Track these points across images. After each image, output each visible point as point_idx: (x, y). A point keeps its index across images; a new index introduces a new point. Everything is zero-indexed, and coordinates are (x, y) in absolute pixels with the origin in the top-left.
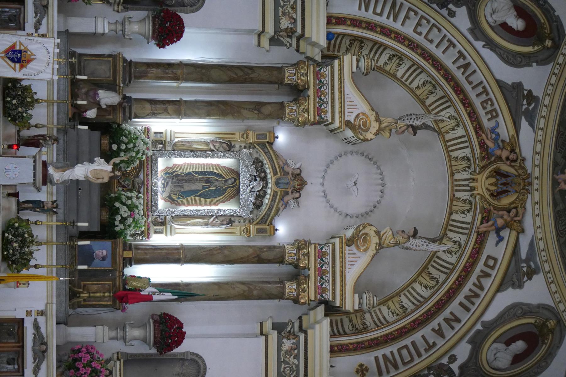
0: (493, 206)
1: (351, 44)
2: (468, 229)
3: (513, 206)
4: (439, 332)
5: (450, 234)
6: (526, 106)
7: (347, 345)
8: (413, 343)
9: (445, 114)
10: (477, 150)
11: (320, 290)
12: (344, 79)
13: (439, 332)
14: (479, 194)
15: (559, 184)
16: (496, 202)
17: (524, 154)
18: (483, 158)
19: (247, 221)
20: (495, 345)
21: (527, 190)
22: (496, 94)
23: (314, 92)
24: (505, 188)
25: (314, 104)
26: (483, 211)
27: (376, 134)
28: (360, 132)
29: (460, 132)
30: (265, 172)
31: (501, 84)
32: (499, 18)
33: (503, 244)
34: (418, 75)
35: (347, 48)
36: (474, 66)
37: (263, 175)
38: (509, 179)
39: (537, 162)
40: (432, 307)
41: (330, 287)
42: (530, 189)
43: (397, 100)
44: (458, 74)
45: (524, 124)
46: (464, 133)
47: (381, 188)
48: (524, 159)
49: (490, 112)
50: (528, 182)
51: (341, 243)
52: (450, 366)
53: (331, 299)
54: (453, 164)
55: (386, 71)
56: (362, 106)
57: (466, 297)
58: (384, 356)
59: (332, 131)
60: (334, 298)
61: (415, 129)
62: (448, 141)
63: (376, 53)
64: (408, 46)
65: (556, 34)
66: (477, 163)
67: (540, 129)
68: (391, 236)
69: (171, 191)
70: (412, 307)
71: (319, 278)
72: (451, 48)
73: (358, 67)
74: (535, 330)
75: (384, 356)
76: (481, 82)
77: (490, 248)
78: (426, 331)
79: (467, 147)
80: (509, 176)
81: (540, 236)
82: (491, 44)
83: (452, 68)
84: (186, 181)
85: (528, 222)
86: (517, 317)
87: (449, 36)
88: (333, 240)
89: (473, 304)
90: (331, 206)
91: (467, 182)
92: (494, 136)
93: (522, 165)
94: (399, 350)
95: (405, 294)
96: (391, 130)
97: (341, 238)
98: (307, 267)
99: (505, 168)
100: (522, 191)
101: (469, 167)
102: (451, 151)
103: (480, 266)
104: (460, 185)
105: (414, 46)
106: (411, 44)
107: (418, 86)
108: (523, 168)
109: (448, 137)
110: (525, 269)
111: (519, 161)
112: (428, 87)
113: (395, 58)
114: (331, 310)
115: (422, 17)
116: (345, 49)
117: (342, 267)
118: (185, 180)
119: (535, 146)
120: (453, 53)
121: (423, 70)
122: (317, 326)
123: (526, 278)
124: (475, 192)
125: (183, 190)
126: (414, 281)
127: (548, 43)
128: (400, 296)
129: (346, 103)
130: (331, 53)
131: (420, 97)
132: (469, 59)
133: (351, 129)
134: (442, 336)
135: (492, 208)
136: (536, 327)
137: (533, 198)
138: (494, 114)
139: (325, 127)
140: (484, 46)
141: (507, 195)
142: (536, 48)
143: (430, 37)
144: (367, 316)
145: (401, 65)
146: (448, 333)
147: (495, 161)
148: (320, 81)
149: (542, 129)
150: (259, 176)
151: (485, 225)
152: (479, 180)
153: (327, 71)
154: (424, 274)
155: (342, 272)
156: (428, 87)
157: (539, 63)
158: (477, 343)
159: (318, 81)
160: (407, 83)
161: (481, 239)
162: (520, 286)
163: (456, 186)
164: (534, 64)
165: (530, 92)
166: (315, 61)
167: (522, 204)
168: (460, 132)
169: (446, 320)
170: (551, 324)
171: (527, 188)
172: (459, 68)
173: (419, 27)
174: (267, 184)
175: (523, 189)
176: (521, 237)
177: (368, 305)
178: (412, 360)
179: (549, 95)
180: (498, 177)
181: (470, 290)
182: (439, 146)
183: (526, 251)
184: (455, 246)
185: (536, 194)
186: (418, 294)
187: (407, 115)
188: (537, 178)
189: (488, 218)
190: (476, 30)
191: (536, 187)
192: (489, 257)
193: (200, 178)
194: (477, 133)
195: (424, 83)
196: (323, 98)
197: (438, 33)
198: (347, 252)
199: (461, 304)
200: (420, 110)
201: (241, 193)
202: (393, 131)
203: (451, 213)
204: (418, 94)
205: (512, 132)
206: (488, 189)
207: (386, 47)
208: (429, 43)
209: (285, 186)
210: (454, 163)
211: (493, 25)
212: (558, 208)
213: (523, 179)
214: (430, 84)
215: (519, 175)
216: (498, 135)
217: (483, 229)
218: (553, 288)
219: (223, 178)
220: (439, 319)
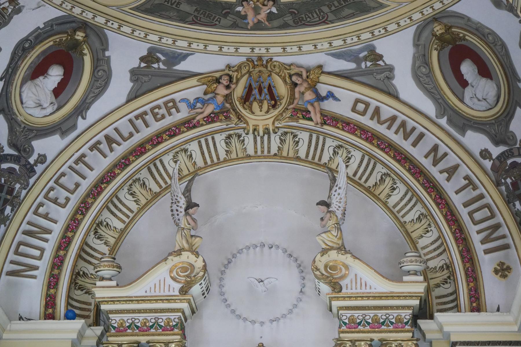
0: (288, 105)
1: (81, 288)
2: (317, 139)
3: (288, 80)
4: (451, 171)
5: (325, 159)
6: (161, 64)
7: (470, 290)
8: (466, 205)
9: (171, 167)
10: (216, 126)
11: (398, 325)
12: (126, 297)
13: (451, 171)
14: (273, 123)
15: (259, 22)
16: (284, 101)
17: (223, 67)
18: (227, 118)
20: (467, 100)
21: (267, 62)
22: (145, 102)
23: (143, 335)
24: (266, 91)
25: (159, 335)
26: (296, 117)
27: (197, 255)
28: (194, 276)
29: (193, 147)
31: (132, 97)
32: (47, 98)
33: (337, 92)
34: (121, 202)
35: (86, 293)
36: (110, 131)
38: (254, 85)
39: (232, 50)
40: (418, 181)
41: (395, 313)
42: (266, 58)
43: (152, 228)
44: (120, 150)
45: (182, 66)
47: (266, 248)
48: (229, 67)
49: (168, 110)
50: (257, 61)
51: (337, 298)
52: (494, 157)
53: (411, 311)
54: (235, 157)
55: (116, 243)
56: (162, 272)
57: (406, 138)
58: (483, 242)
59: (193, 312)
60: (408, 307)
61: (191, 205)
62: (206, 163)
63: (92, 256)
64: (84, 215)
65: (68, 25)
67: (189, 46)
68: (329, 234)
70: (419, 206)
71: (383, 327)
72: (86, 159)
73: (110, 279)
74: (447, 50)
75: (483, 242)
76: (130, 121)
77: (342, 108)
78: (449, 188)
79: (213, 138)
80: (250, 85)
81: (326, 46)
82: (81, 110)
83: (112, 158)
85: (310, 60)
86: (430, 73)
87: (70, 162)
88: (335, 310)
89: (414, 129)
90: (290, 312)
91: (259, 139)
92: (199, 105)
93: (236, 68)
94: (475, 223)
95: (403, 217)
96: (192, 236)
97: (331, 299)
98: (369, 343)
99: (239, 90)
100: (269, 69)
101: (239, 136)
102: (218, 159)
103: (365, 121)
104: (262, 148)
105: (83, 207)
106: (82, 211)
107: (135, 201)
108: (240, 67)
109: (200, 163)
110: (369, 64)
111: (231, 73)
112: (137, 188)
113: (99, 231)
114: (424, 312)
115: (46, 197)
116: (87, 295)
117: (368, 298)
119: (212, 53)
120: (92, 157)
121: (115, 195)
122: (446, 329)
123: (381, 63)
126: (385, 204)
127: (80, 36)
128: (405, 222)
129: (157, 293)
130: (92, 314)
131: (149, 198)
132: (101, 137)
133: (191, 288)
134: (456, 168)
135: (292, 106)
136: (442, 48)
137: (278, 55)
138: (171, 104)
139: (189, 321)
140: (84, 118)
141: (274, 87)
142: (86, 51)
143: (72, 187)
144: (431, 264)
145: (107, 224)
146: (452, 160)
147: (231, 104)
148: (129, 327)
151: (312, 115)
152: (255, 123)
153: (115, 319)
154: (377, 193)
155: (375, 298)
156: (137, 188)
157: (106, 48)
158: (464, 123)
159: (129, 331)
160: (131, 215)
161: (331, 119)
162: (391, 69)
163: (263, 152)
164: (107, 54)
165: (142, 59)
166: (102, 335)
167: (286, 69)
168: (193, 147)
169: (435, 163)
170: (438, 29)
171: (265, 62)
172: (112, 150)
173: (59, 201)
175: (266, 67)
176: (326, 69)
177: (418, 264)
178: (488, 206)
179: (147, 35)
180: (252, 99)
181: (396, 133)
182: (211, 175)
184: (340, 152)
185: (272, 50)
186: (402, 199)
187: (173, 215)
188: (253, 49)
189: (304, 111)
190: (63, 128)
191: (263, 51)
192: (354, 110)
194: (195, 127)
195: (131, 194)
196: (151, 324)
197: (66, 177)
198: (349, 291)
199: (414, 144)
200: (165, 200)
202: (193, 233)
203: (298, 159)
204: (146, 201)
205: (193, 81)
206: (267, 112)
207: (85, 243)
208: (79, 188)
210: (234, 156)
211: (56, 107)
212: (291, 22)
213: (254, 67)
214: (133, 186)
215: (249, 72)
216: (197, 99)
217: (317, 118)
218: (392, 27)
220: (434, 172)
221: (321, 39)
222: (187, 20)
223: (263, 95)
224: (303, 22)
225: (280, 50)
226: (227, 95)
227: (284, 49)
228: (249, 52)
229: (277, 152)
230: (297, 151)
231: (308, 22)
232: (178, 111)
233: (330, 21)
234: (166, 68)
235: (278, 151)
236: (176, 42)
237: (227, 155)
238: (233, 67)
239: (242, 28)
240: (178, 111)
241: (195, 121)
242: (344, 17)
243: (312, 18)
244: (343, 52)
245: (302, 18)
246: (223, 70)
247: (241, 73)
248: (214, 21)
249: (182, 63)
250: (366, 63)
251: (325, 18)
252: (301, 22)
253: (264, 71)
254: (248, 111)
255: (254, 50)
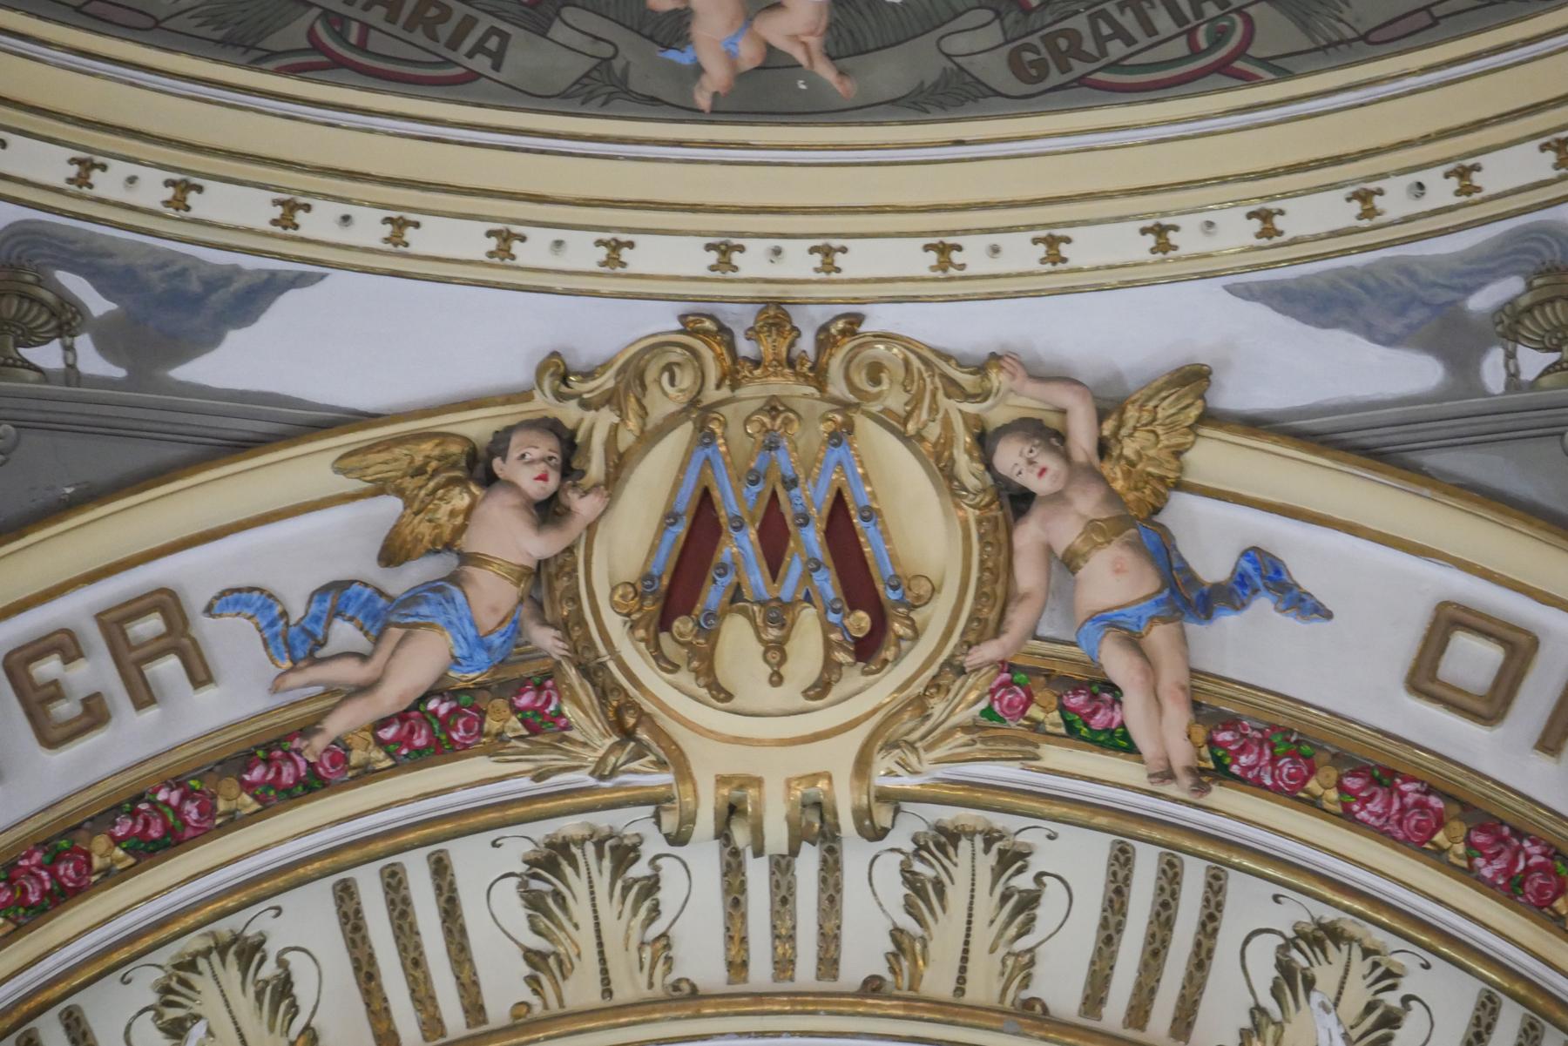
0: (968, 644)
3: (967, 467)
14: (862, 765)
15: (774, 61)
16: (935, 617)
17: (518, 373)
18: (543, 726)
21: (825, 340)
24: (812, 538)
26: (1015, 726)
33: (1308, 554)
38: (729, 502)
39: (584, 252)
42: (820, 314)
45: (236, 363)
46: (323, 891)
48: (558, 371)
50: (752, 334)
66: (582, 778)
77: (1341, 665)
79: (440, 867)
80: (705, 499)
81: (1237, 231)
85: (1118, 332)
91: (757, 873)
92: (344, 634)
93: (607, 381)
99: (627, 536)
100: (838, 388)
101: (625, 854)
104: (784, 936)
108: (633, 375)
110: (1532, 362)
111: (569, 413)
119: (443, 273)
124: (845, 802)
135: (990, 651)
138: (152, 625)
141: (870, 514)
147: (570, 627)
149: (290, 209)
151: (1134, 712)
152: (738, 762)
161: (1256, 744)
163: (784, 965)
167: (953, 388)
168: (303, 927)
171: (807, 343)
175: (818, 375)
176: (1231, 396)
180: (713, 595)
183: (1372, 353)
184: (1326, 976)
185: (860, 260)
188: (725, 250)
189: (1076, 687)
191: (799, 262)
192: (1423, 679)
194: (313, 784)
206: (820, 689)
210: (582, 990)
213: (732, 377)
215: (699, 412)
217: (1166, 731)
221: (1202, 183)
222: (274, 42)
223: (794, 568)
224: (1079, 68)
225: (914, 259)
226: (542, 564)
227: (943, 250)
228: (703, 271)
229: (882, 969)
230: (1025, 965)
231: (1115, 66)
232: (200, 675)
233: (1263, 62)
234: (120, 373)
235: (893, 959)
236: (192, 198)
237: (533, 982)
238: (588, 375)
239: (654, 101)
240: (200, 675)
241: (319, 742)
242: (1364, 38)
243: (1144, 41)
244: (1349, 274)
245: (1074, 36)
246: (524, 396)
247: (644, 412)
248: (459, 55)
249: (235, 339)
250: (1510, 356)
251: (1234, 41)
252: (1065, 69)
253: (801, 406)
254: (685, 678)
255: (736, 257)
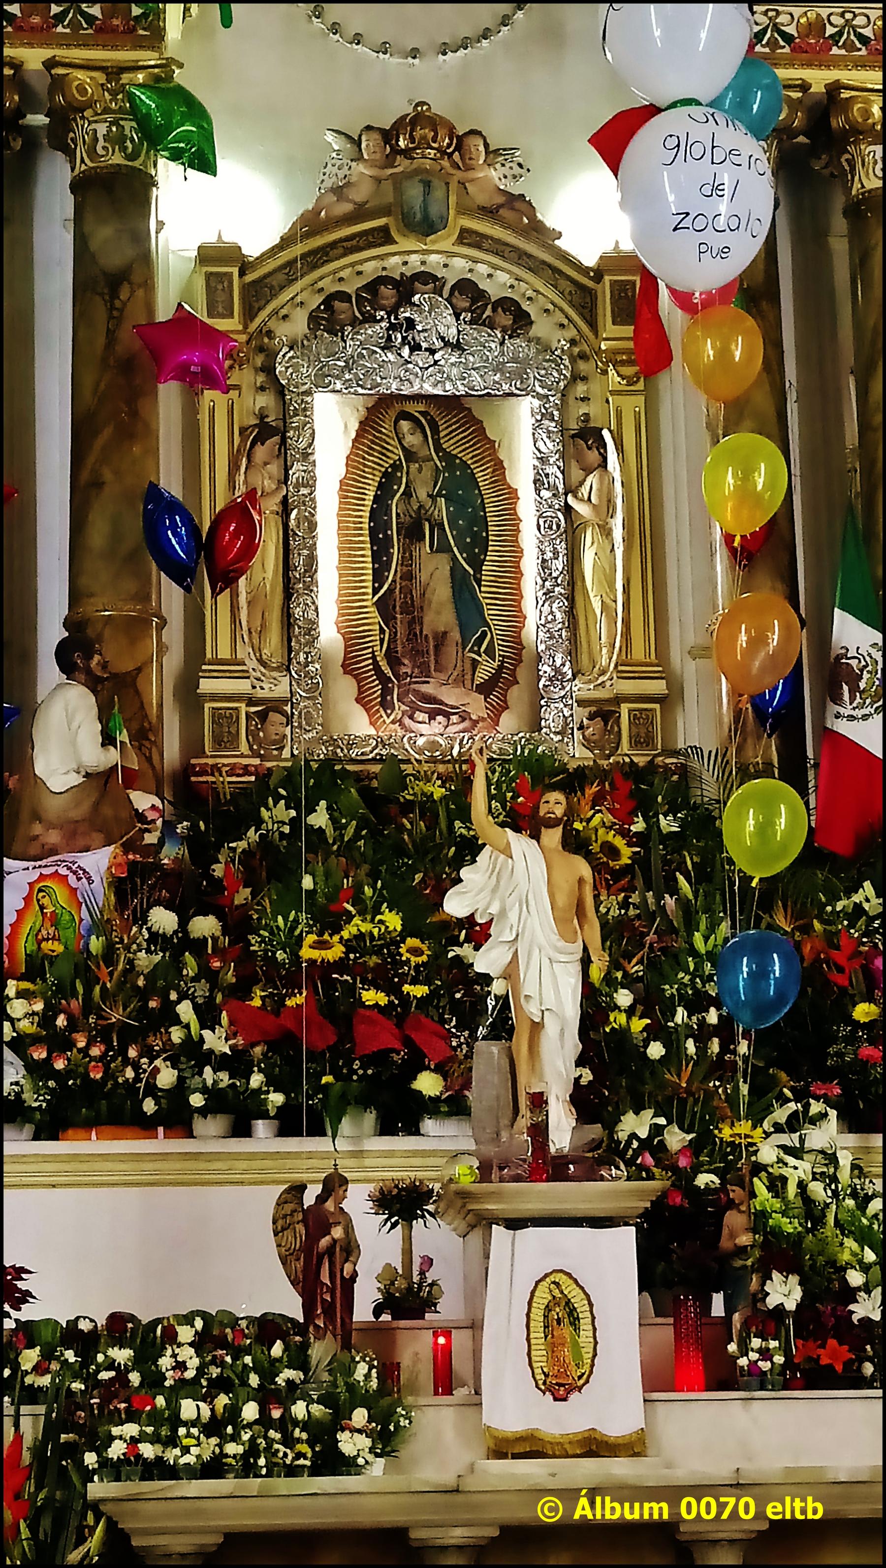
19: (583, 367)
30: (373, 286)
37: (388, 293)
69: (460, 681)
84: (415, 622)
118: (411, 623)
125: (456, 635)
150: (393, 311)
174: (425, 277)
193: (402, 562)
201: (462, 390)
209: (438, 193)
219: (396, 467)
